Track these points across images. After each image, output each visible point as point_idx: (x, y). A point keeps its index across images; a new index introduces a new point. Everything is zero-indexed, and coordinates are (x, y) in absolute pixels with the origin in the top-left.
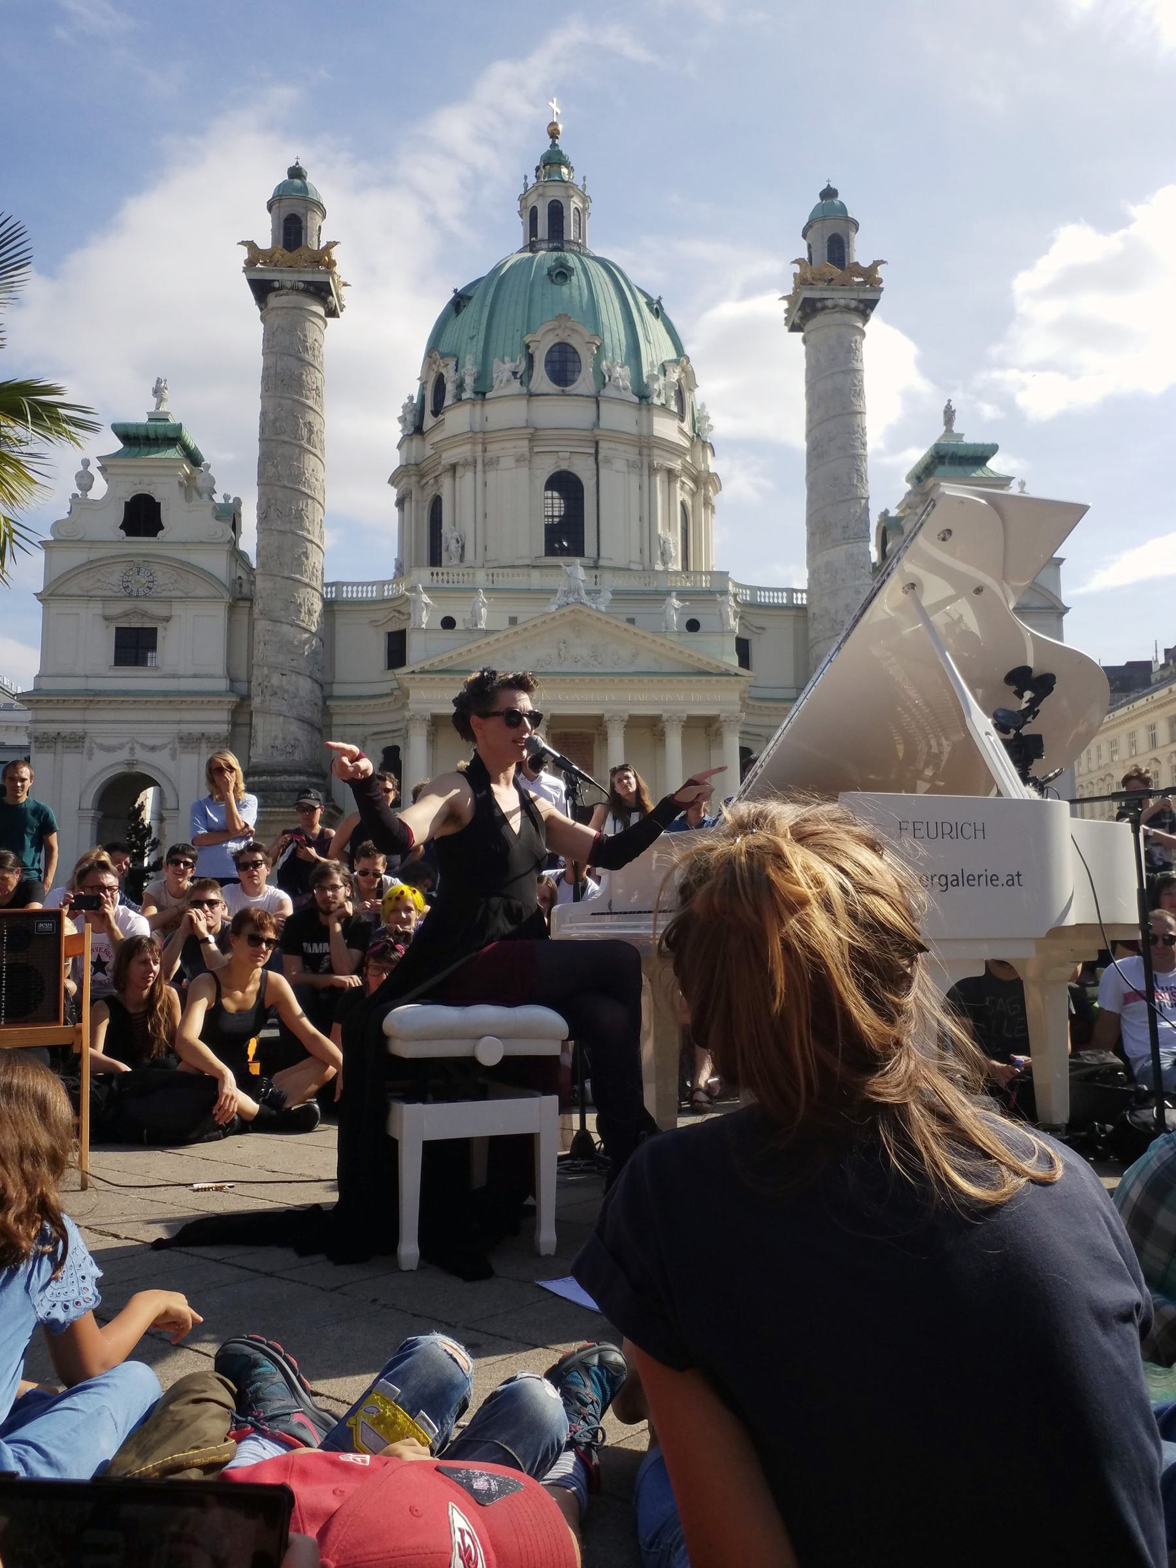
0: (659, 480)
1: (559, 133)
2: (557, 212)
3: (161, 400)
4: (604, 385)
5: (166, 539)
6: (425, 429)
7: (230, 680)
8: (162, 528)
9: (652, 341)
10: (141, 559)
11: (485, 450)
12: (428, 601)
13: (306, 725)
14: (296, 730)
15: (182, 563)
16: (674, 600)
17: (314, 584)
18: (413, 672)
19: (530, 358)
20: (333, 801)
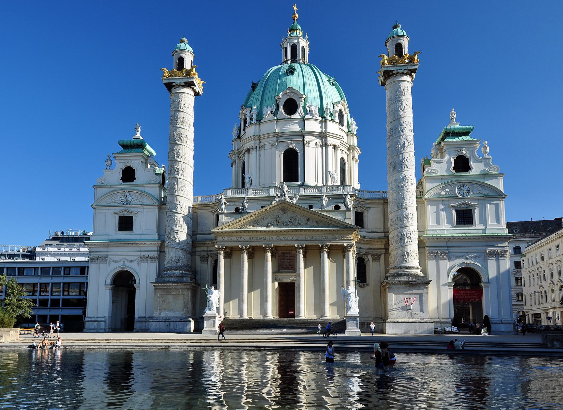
0: (330, 149)
2: (294, 48)
3: (138, 131)
5: (137, 183)
7: (159, 235)
8: (135, 179)
9: (328, 95)
12: (225, 201)
13: (184, 251)
14: (180, 254)
15: (142, 191)
16: (324, 197)
17: (188, 197)
18: (218, 230)
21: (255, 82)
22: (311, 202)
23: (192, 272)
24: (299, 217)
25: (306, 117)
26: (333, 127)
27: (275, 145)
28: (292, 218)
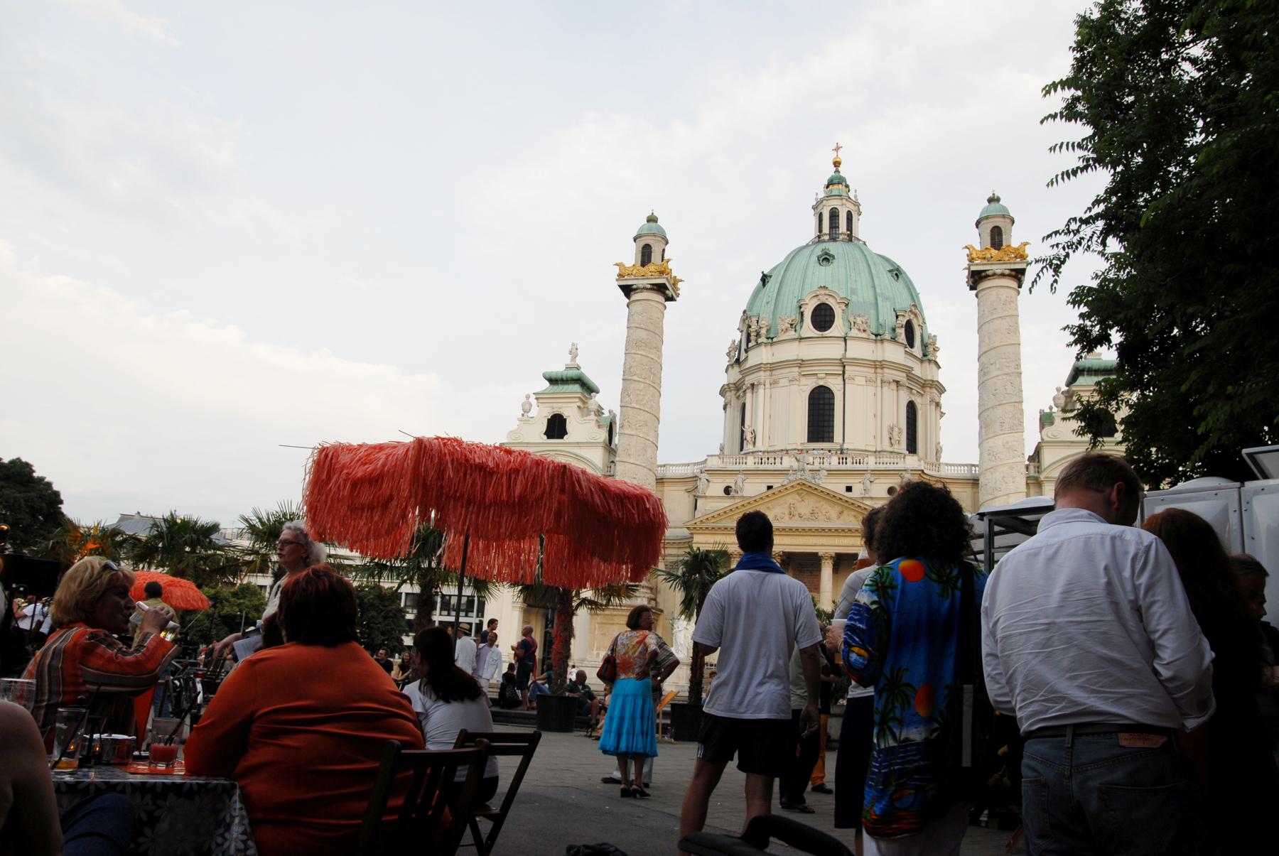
1: (840, 163)
2: (834, 215)
4: (851, 329)
5: (568, 441)
6: (741, 360)
8: (566, 433)
10: (554, 453)
11: (771, 375)
15: (576, 455)
19: (802, 314)
20: (657, 603)
21: (765, 273)
22: (849, 481)
23: (651, 589)
24: (827, 506)
25: (849, 335)
26: (894, 353)
27: (796, 380)
28: (817, 508)
